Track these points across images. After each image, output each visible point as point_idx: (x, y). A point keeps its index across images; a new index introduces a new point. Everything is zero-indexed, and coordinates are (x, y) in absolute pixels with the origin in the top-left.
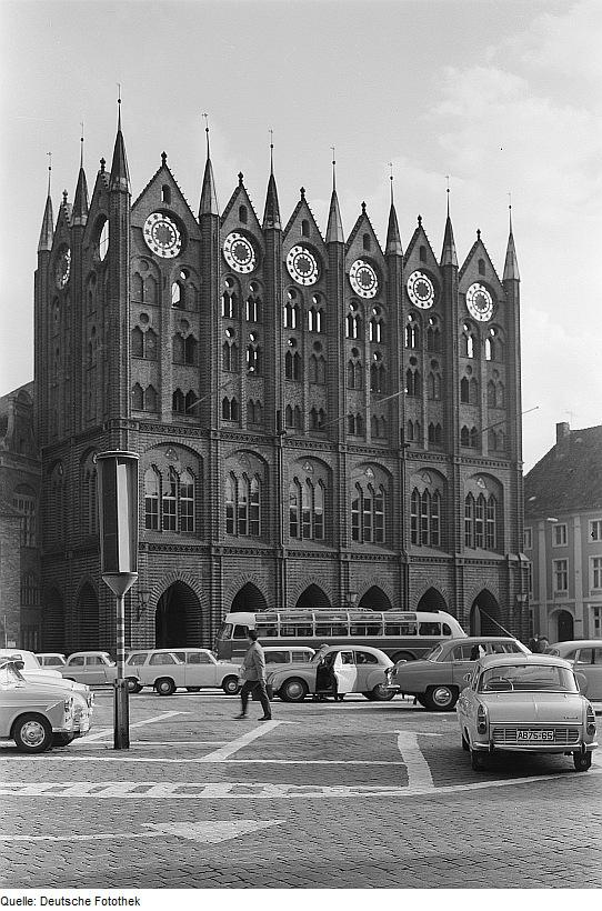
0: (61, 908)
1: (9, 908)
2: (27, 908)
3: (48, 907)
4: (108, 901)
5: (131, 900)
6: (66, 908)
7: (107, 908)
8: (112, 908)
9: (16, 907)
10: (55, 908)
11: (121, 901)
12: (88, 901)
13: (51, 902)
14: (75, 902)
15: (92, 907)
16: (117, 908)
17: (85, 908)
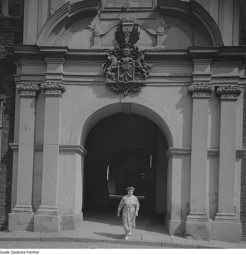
0: (17, 254)
1: (2, 254)
2: (8, 254)
3: (13, 254)
4: (30, 252)
5: (37, 252)
6: (18, 254)
7: (30, 254)
8: (31, 254)
9: (4, 254)
10: (15, 254)
11: (34, 252)
12: (25, 252)
13: (14, 252)
14: (21, 253)
15: (26, 254)
16: (33, 254)
17: (24, 254)
